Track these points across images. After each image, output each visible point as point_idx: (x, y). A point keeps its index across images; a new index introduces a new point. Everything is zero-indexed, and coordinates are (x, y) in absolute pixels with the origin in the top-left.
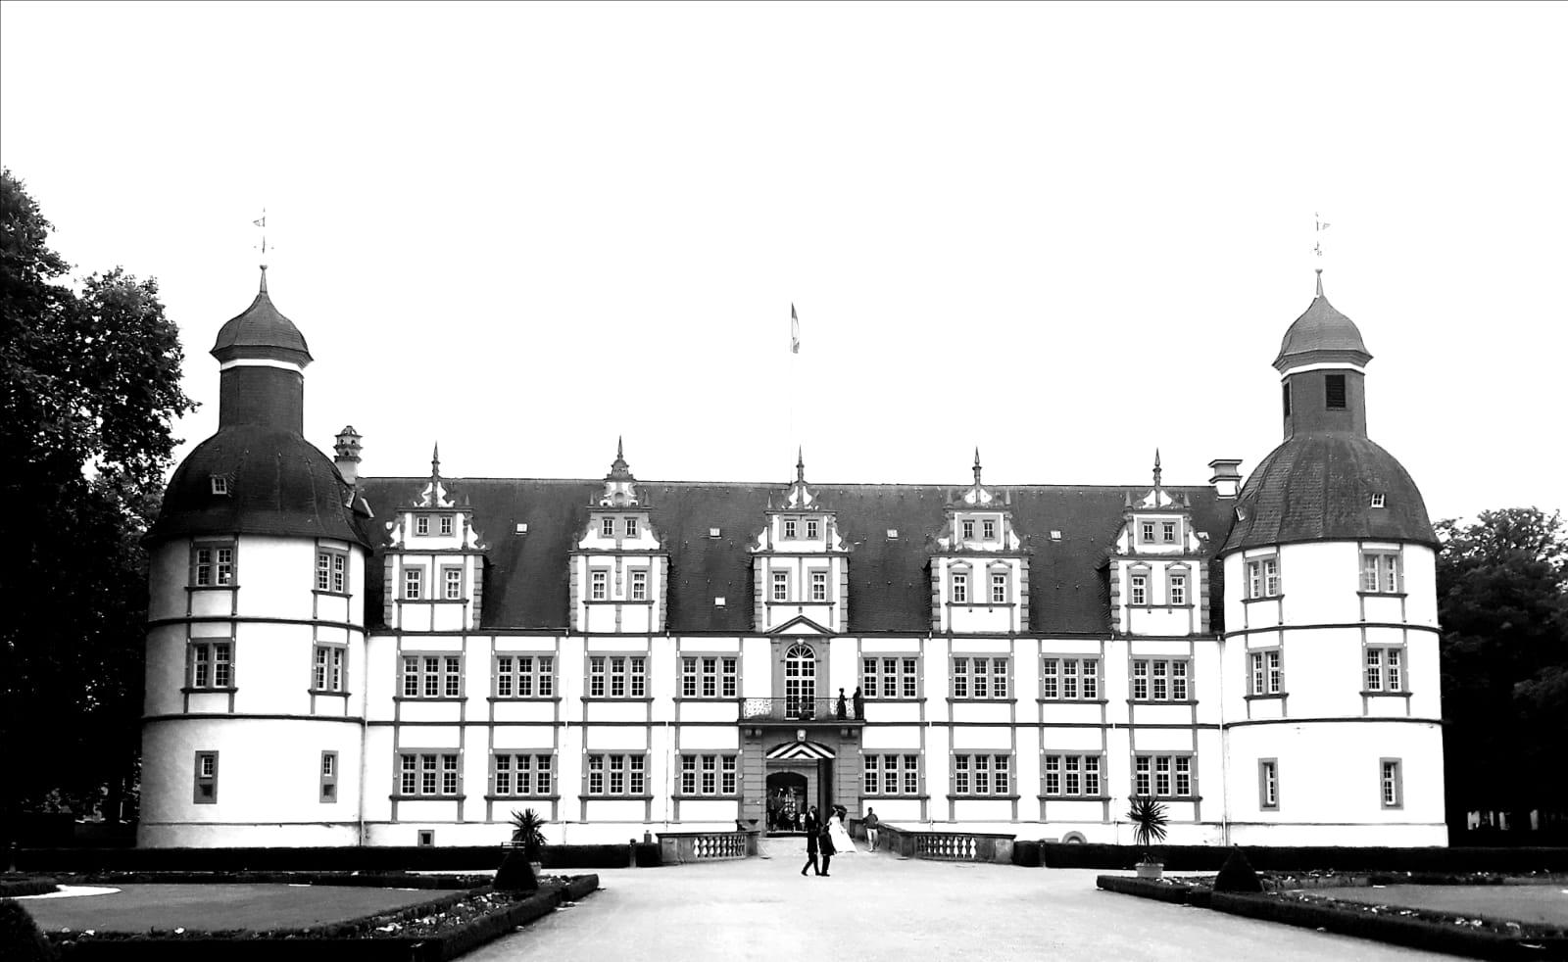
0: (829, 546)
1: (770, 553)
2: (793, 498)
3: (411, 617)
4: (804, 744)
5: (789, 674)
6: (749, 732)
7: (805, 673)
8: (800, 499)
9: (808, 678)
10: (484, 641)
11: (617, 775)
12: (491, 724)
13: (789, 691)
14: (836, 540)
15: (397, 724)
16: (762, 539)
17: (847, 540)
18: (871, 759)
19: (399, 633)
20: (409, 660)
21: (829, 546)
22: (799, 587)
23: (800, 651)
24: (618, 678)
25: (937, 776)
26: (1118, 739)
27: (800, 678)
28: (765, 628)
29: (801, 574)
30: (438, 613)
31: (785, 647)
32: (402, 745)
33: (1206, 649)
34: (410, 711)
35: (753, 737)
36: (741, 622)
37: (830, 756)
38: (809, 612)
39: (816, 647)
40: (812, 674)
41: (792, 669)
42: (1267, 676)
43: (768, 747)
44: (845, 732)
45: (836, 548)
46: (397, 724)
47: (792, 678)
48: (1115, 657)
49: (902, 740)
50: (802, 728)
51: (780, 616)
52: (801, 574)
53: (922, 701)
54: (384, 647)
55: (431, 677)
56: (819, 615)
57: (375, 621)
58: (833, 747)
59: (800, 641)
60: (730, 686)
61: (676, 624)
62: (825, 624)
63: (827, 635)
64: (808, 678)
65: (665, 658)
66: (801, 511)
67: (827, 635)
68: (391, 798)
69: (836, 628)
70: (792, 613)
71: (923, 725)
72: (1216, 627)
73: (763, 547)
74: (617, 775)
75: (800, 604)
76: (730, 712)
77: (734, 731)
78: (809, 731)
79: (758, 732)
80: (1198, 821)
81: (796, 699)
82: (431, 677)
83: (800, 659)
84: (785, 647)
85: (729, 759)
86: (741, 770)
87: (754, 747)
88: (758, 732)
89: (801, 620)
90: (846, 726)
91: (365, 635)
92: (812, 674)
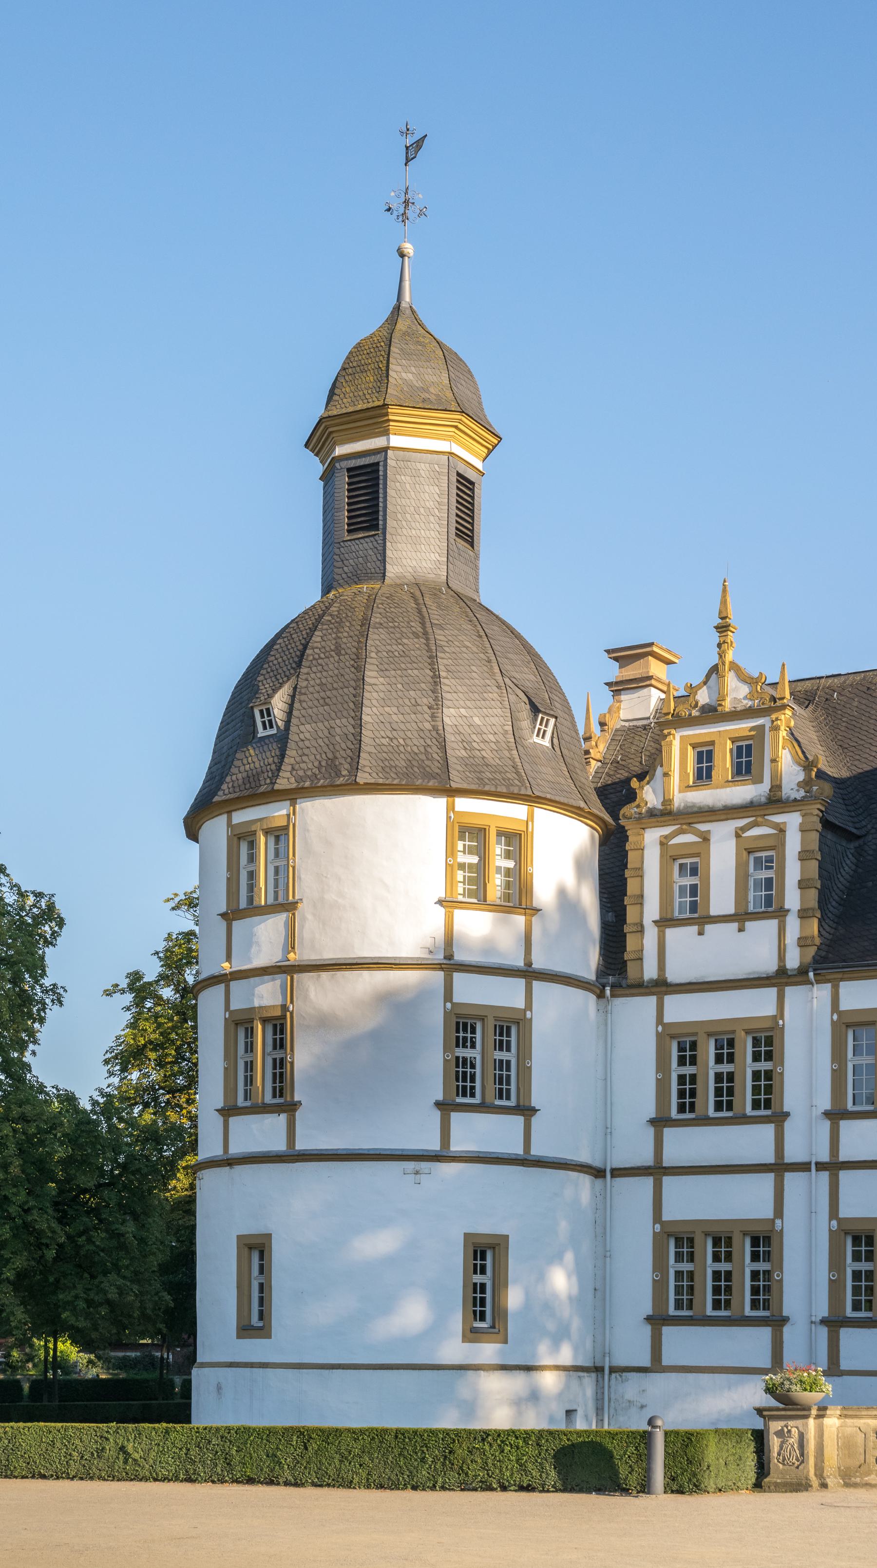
3: (688, 953)
10: (821, 993)
12: (834, 1167)
15: (657, 1171)
20: (682, 1044)
32: (667, 1215)
34: (686, 1144)
54: (637, 1016)
57: (615, 970)
82: (718, 1075)
91: (601, 996)
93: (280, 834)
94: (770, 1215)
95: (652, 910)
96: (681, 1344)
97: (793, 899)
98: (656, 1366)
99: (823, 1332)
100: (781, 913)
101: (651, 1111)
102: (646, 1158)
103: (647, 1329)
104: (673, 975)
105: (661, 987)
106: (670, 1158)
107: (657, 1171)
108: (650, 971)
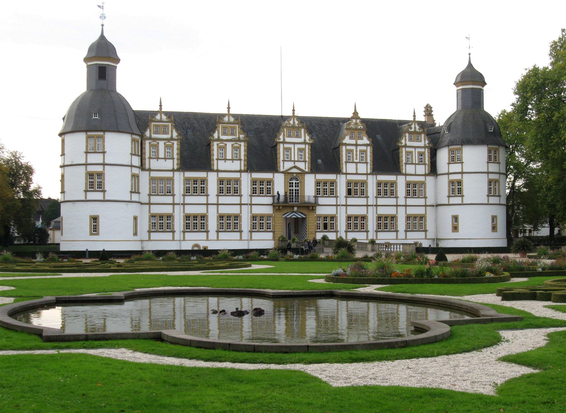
0: (305, 140)
1: (284, 142)
2: (291, 122)
3: (154, 164)
4: (295, 212)
5: (290, 186)
6: (277, 208)
7: (296, 186)
8: (294, 122)
9: (297, 188)
11: (229, 223)
12: (184, 204)
13: (290, 193)
14: (308, 138)
16: (281, 137)
17: (311, 138)
18: (319, 217)
19: (150, 170)
21: (305, 140)
22: (295, 155)
23: (294, 179)
24: (228, 187)
25: (342, 224)
26: (401, 210)
27: (294, 188)
28: (282, 170)
29: (294, 151)
30: (165, 163)
31: (289, 177)
33: (430, 180)
34: (154, 199)
35: (279, 209)
36: (273, 167)
37: (304, 217)
38: (297, 164)
39: (300, 176)
40: (298, 187)
41: (291, 185)
42: (456, 188)
43: (284, 213)
44: (311, 208)
45: (307, 141)
46: (150, 204)
47: (291, 188)
48: (401, 181)
49: (330, 211)
50: (296, 206)
51: (288, 165)
52: (294, 151)
53: (337, 197)
55: (162, 187)
56: (301, 165)
57: (142, 167)
58: (306, 213)
59: (295, 175)
60: (269, 191)
61: (251, 167)
62: (303, 168)
63: (303, 173)
64: (297, 188)
65: (246, 180)
66: (293, 127)
67: (303, 173)
68: (148, 231)
69: (307, 170)
70: (291, 164)
71: (337, 205)
72: (433, 170)
73: (282, 140)
74: (229, 223)
75: (294, 161)
76: (269, 200)
77: (271, 207)
78: (298, 207)
79: (281, 208)
80: (426, 238)
81: (293, 196)
82: (162, 187)
83: (294, 182)
84: (289, 177)
85: (269, 217)
86: (274, 221)
87: (278, 213)
88: (281, 208)
89: (295, 167)
90: (311, 207)
92: (298, 187)
93: (102, 137)
94: (171, 212)
95: (147, 155)
96: (154, 236)
97: (175, 156)
98: (150, 239)
99: (182, 234)
100: (173, 159)
101: (148, 193)
102: (147, 201)
103: (148, 234)
104: (152, 168)
105: (150, 170)
106: (152, 202)
107: (150, 204)
108: (147, 167)
